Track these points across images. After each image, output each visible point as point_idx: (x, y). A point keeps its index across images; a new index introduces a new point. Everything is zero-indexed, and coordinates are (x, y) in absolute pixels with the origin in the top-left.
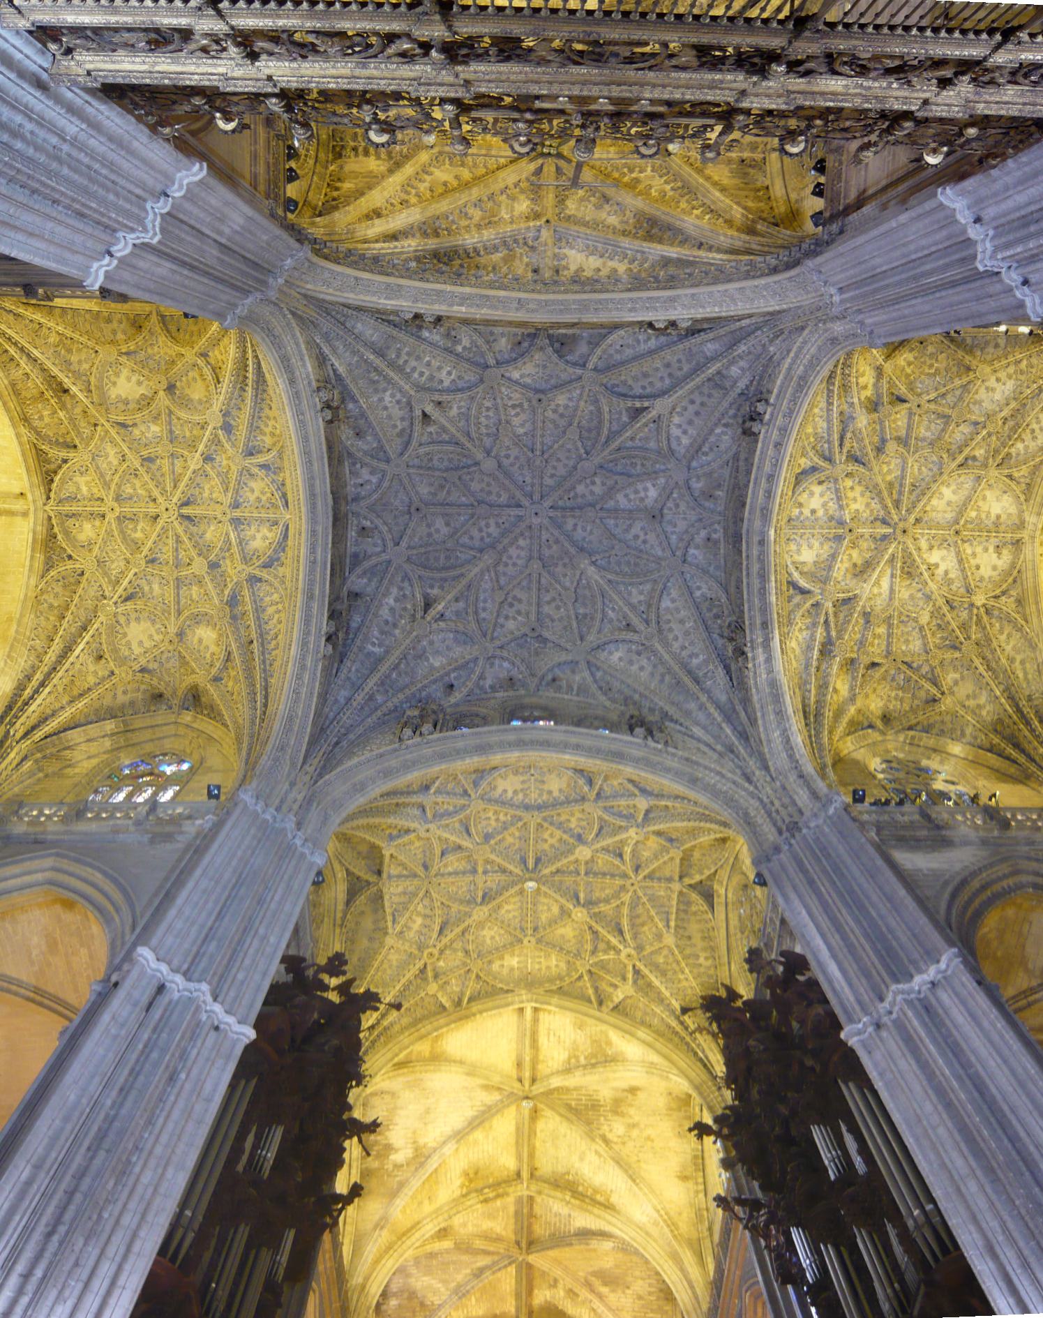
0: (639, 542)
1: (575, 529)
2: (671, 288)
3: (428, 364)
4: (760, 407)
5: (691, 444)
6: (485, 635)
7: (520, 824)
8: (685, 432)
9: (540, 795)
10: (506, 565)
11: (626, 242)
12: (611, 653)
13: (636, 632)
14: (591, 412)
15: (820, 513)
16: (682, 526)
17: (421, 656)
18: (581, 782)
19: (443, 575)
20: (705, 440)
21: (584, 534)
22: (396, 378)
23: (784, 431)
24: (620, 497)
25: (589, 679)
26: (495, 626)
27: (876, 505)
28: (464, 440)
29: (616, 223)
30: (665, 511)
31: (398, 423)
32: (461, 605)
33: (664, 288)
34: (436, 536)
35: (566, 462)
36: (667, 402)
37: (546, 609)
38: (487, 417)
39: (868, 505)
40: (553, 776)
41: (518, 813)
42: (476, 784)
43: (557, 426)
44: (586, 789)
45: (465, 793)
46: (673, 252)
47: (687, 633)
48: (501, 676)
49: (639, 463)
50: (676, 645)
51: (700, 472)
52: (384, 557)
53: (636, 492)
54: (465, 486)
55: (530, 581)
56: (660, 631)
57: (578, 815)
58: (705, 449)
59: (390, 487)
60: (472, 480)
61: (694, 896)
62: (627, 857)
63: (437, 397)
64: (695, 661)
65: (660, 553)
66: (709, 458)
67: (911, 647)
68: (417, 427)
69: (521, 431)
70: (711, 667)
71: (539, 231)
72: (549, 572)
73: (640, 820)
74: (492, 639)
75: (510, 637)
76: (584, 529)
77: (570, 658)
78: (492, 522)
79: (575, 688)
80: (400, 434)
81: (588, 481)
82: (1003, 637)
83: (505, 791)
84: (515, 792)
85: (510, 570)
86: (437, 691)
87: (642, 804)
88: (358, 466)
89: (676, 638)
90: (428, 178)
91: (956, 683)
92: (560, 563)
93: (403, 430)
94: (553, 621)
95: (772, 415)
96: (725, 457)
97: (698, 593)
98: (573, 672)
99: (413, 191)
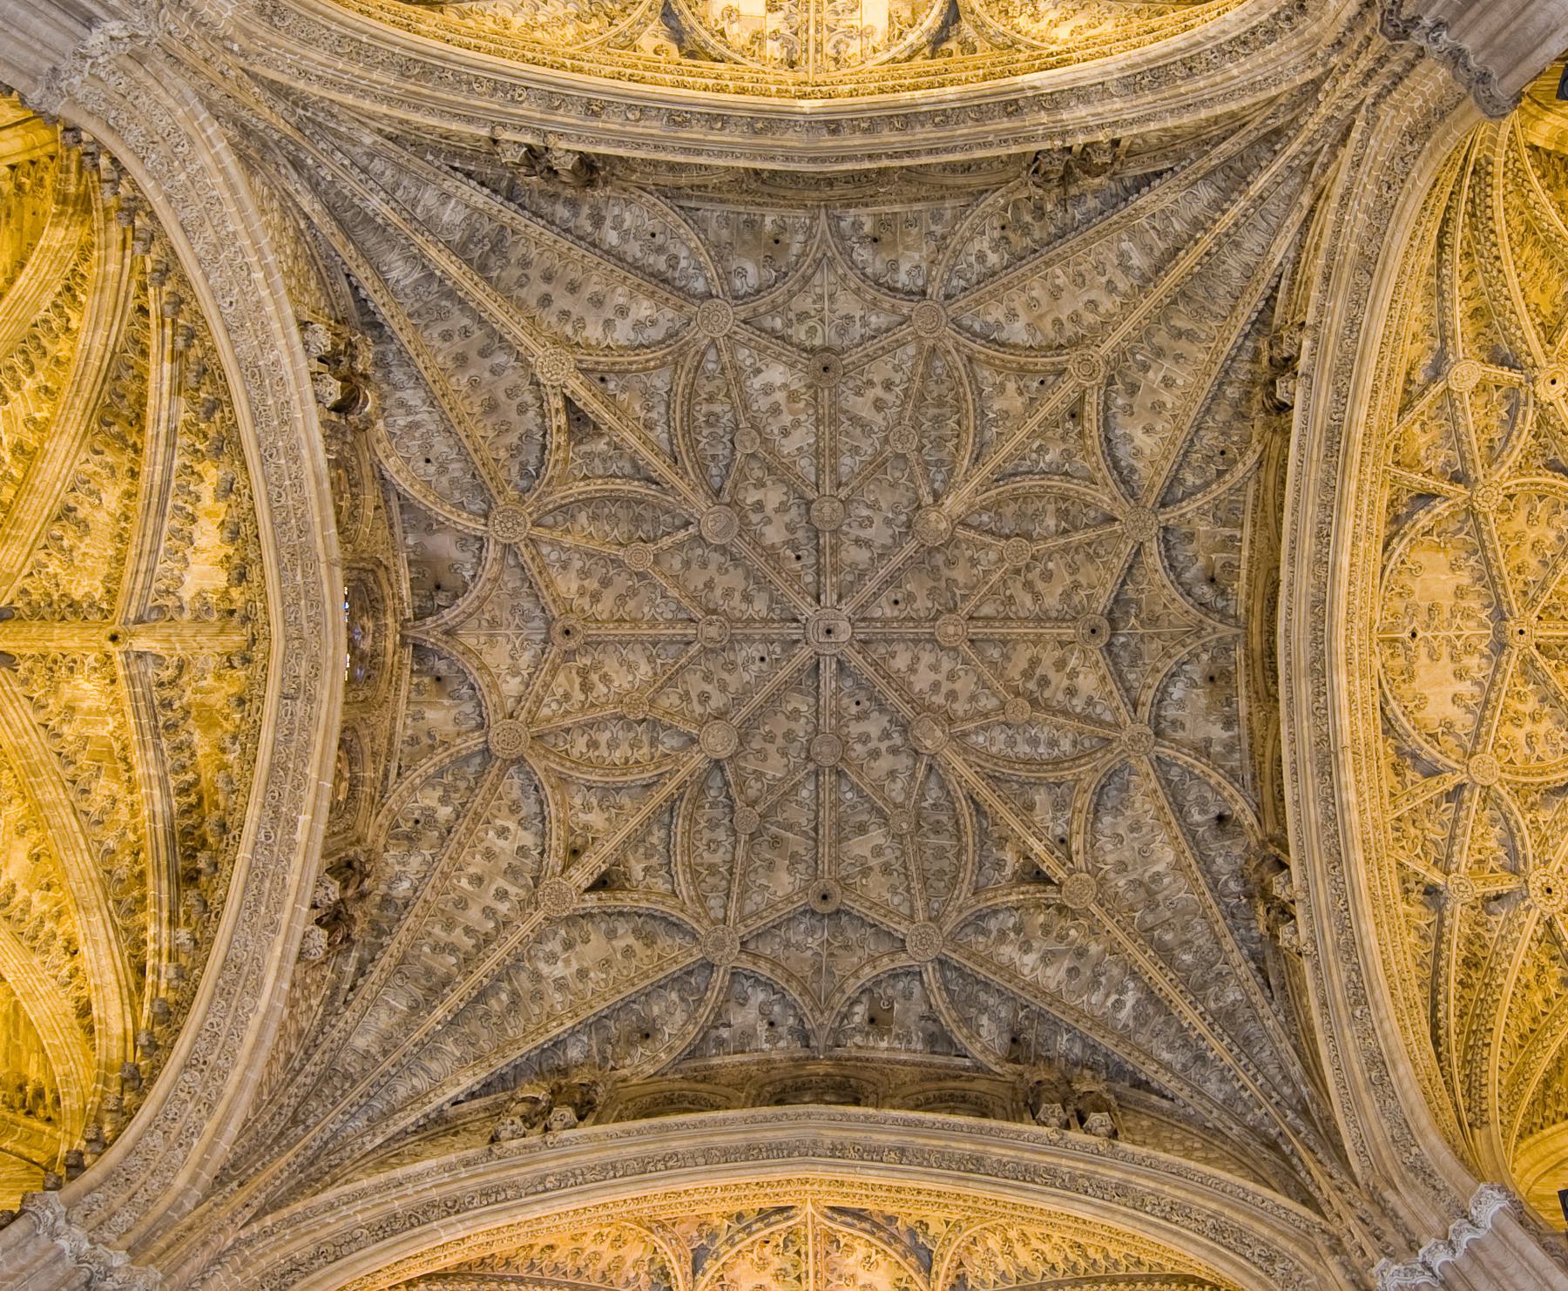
1: (867, 544)
2: (223, 377)
3: (478, 880)
4: (512, 156)
6: (1109, 741)
7: (1541, 661)
8: (622, 311)
10: (952, 695)
11: (153, 472)
12: (1138, 453)
13: (1082, 399)
14: (594, 518)
16: (847, 304)
17: (1149, 890)
20: (636, 267)
21: (878, 520)
22: (499, 954)
23: (554, 98)
24: (789, 446)
25: (1201, 500)
26: (1086, 719)
28: (659, 796)
29: (118, 491)
30: (818, 342)
31: (620, 944)
32: (1041, 797)
33: (227, 391)
34: (889, 855)
35: (712, 567)
36: (542, 356)
37: (1052, 601)
38: (613, 744)
41: (1512, 665)
42: (1432, 772)
45: (1455, 794)
46: (160, 373)
47: (1080, 280)
48: (1203, 702)
49: (705, 408)
50: (1107, 304)
51: (711, 272)
52: (930, 976)
53: (775, 410)
54: (771, 789)
55: (988, 640)
56: (1075, 343)
58: (661, 263)
59: (775, 964)
60: (759, 775)
63: (554, 861)
65: (911, 350)
68: (626, 901)
69: (644, 669)
70: (1143, 221)
71: (140, 656)
72: (964, 597)
73: (1516, 376)
74: (1117, 726)
75: (1111, 686)
76: (867, 522)
77: (1154, 547)
78: (855, 729)
79: (1227, 531)
80: (649, 940)
81: (755, 518)
83: (1456, 699)
84: (1459, 675)
85: (966, 685)
86: (1227, 857)
88: (725, 1033)
89: (1093, 305)
90: (22, 893)
92: (946, 572)
93: (637, 932)
94: (1076, 586)
96: (673, 218)
97: (993, 259)
98: (1190, 537)
99: (49, 925)
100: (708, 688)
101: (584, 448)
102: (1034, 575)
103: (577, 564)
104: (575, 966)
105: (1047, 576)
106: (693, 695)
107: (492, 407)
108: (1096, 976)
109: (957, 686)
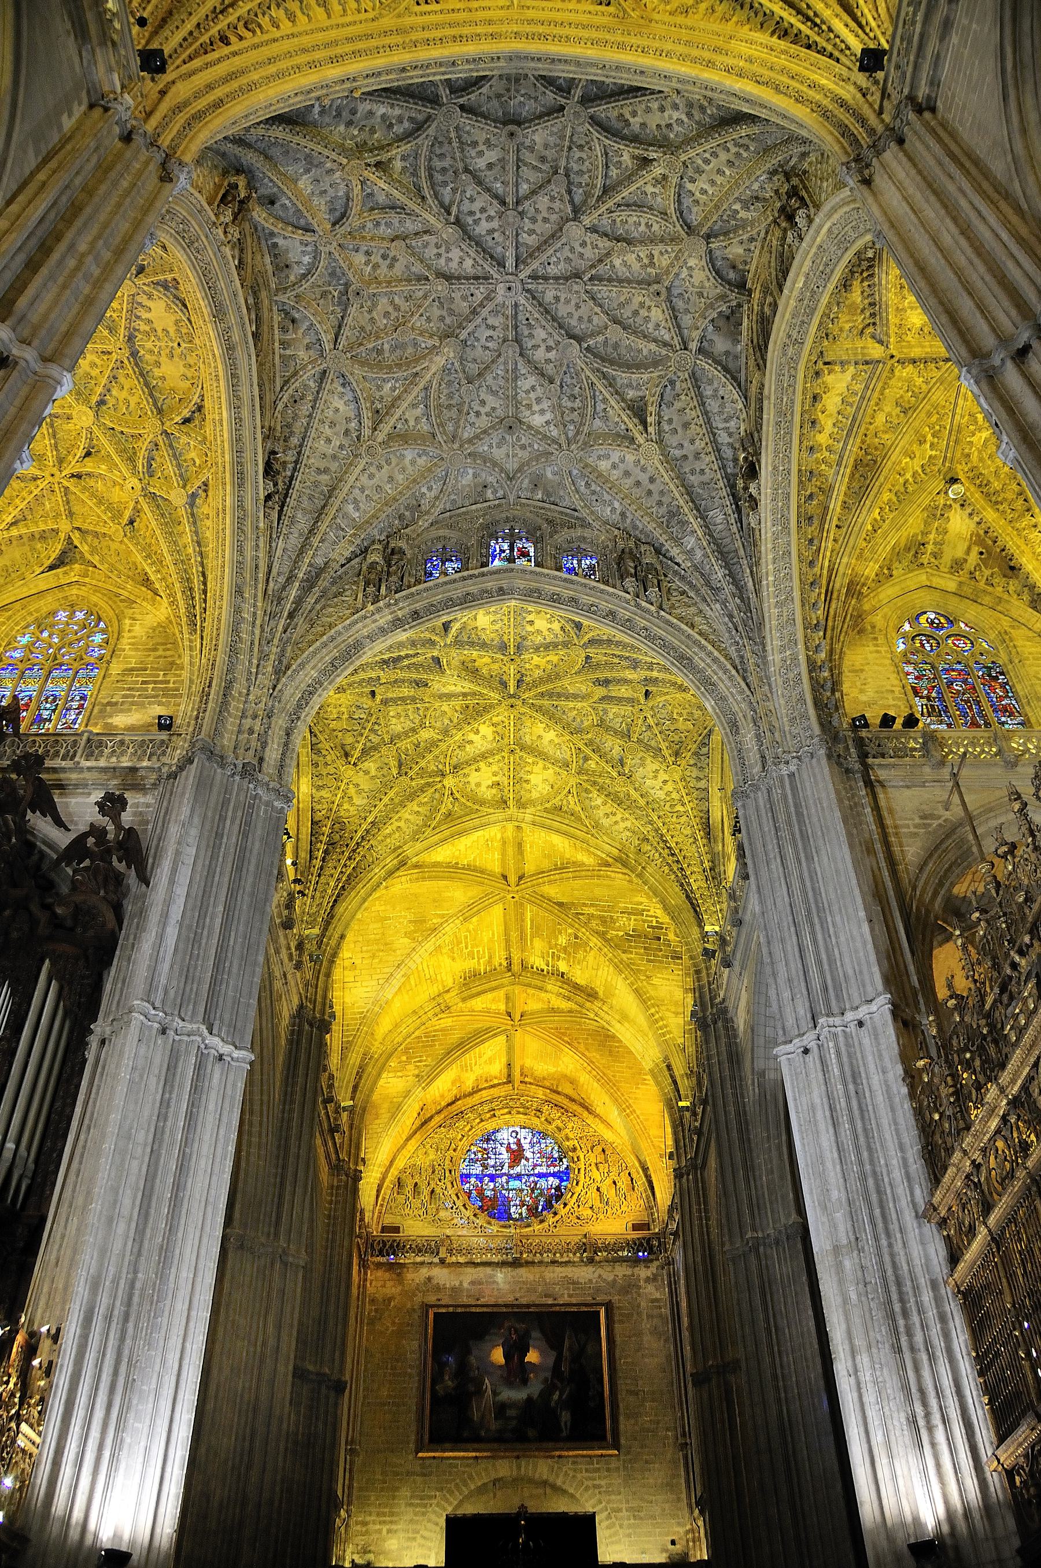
0: (476, 408)
5: (600, 475)
8: (614, 466)
9: (151, 352)
15: (529, 628)
16: (498, 454)
18: (186, 413)
19: (423, 173)
27: (537, 673)
31: (638, 120)
35: (576, 316)
37: (384, 301)
39: (538, 666)
40: (182, 370)
43: (622, 305)
44: (178, 419)
53: (538, 400)
57: (133, 401)
61: (56, 549)
62: (89, 466)
64: (350, 508)
66: (582, 489)
67: (394, 721)
69: (617, 262)
78: (495, 224)
79: (288, 352)
82: (416, 809)
84: (149, 321)
87: (178, 497)
89: (371, 476)
91: (367, 772)
92: (445, 313)
95: (648, 611)
100: (581, 250)
101: (640, 394)
102: (394, 315)
103: (651, 326)
104: (666, 114)
105: (387, 314)
106: (589, 246)
107: (686, 425)
108: (339, 115)
109: (435, 251)
